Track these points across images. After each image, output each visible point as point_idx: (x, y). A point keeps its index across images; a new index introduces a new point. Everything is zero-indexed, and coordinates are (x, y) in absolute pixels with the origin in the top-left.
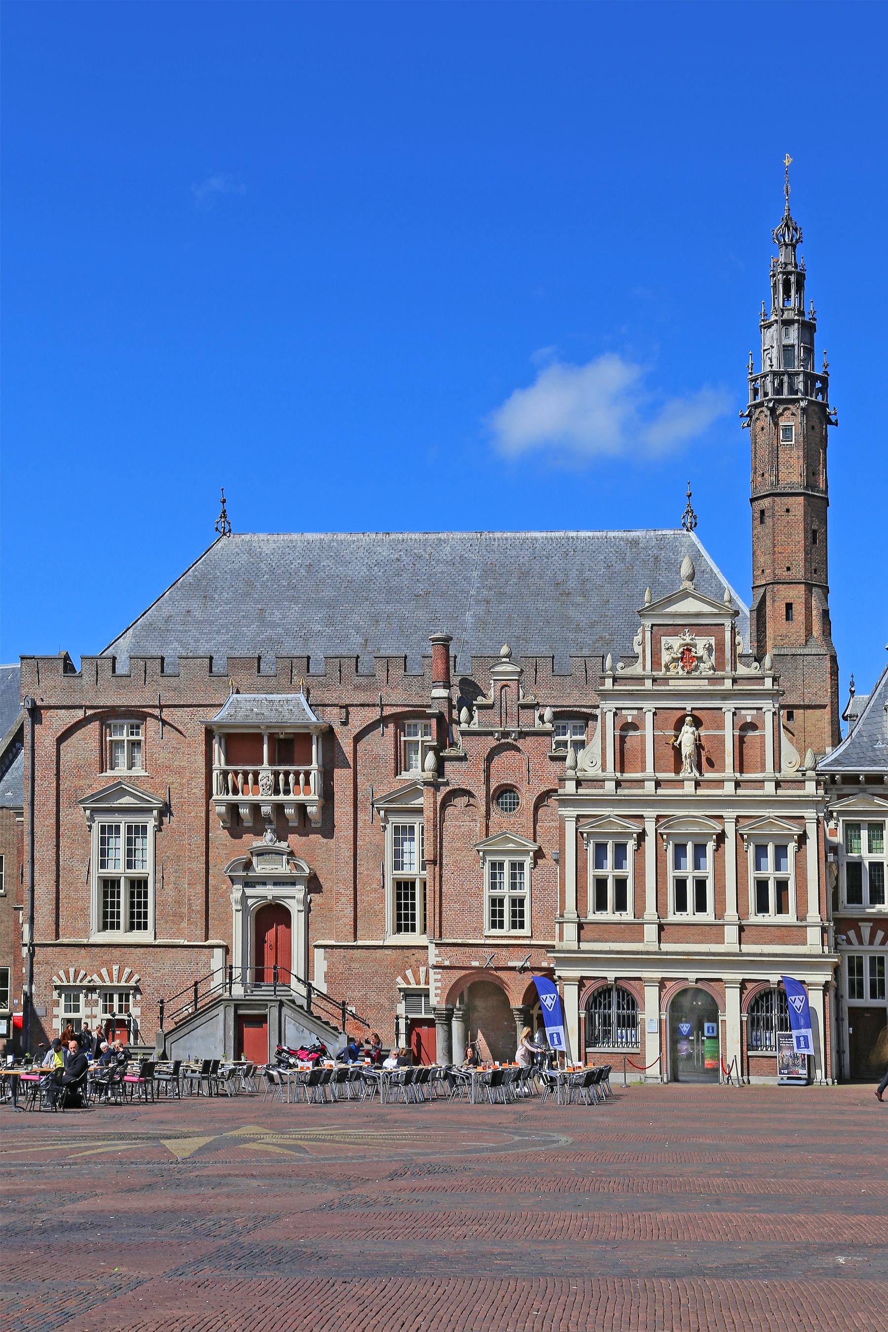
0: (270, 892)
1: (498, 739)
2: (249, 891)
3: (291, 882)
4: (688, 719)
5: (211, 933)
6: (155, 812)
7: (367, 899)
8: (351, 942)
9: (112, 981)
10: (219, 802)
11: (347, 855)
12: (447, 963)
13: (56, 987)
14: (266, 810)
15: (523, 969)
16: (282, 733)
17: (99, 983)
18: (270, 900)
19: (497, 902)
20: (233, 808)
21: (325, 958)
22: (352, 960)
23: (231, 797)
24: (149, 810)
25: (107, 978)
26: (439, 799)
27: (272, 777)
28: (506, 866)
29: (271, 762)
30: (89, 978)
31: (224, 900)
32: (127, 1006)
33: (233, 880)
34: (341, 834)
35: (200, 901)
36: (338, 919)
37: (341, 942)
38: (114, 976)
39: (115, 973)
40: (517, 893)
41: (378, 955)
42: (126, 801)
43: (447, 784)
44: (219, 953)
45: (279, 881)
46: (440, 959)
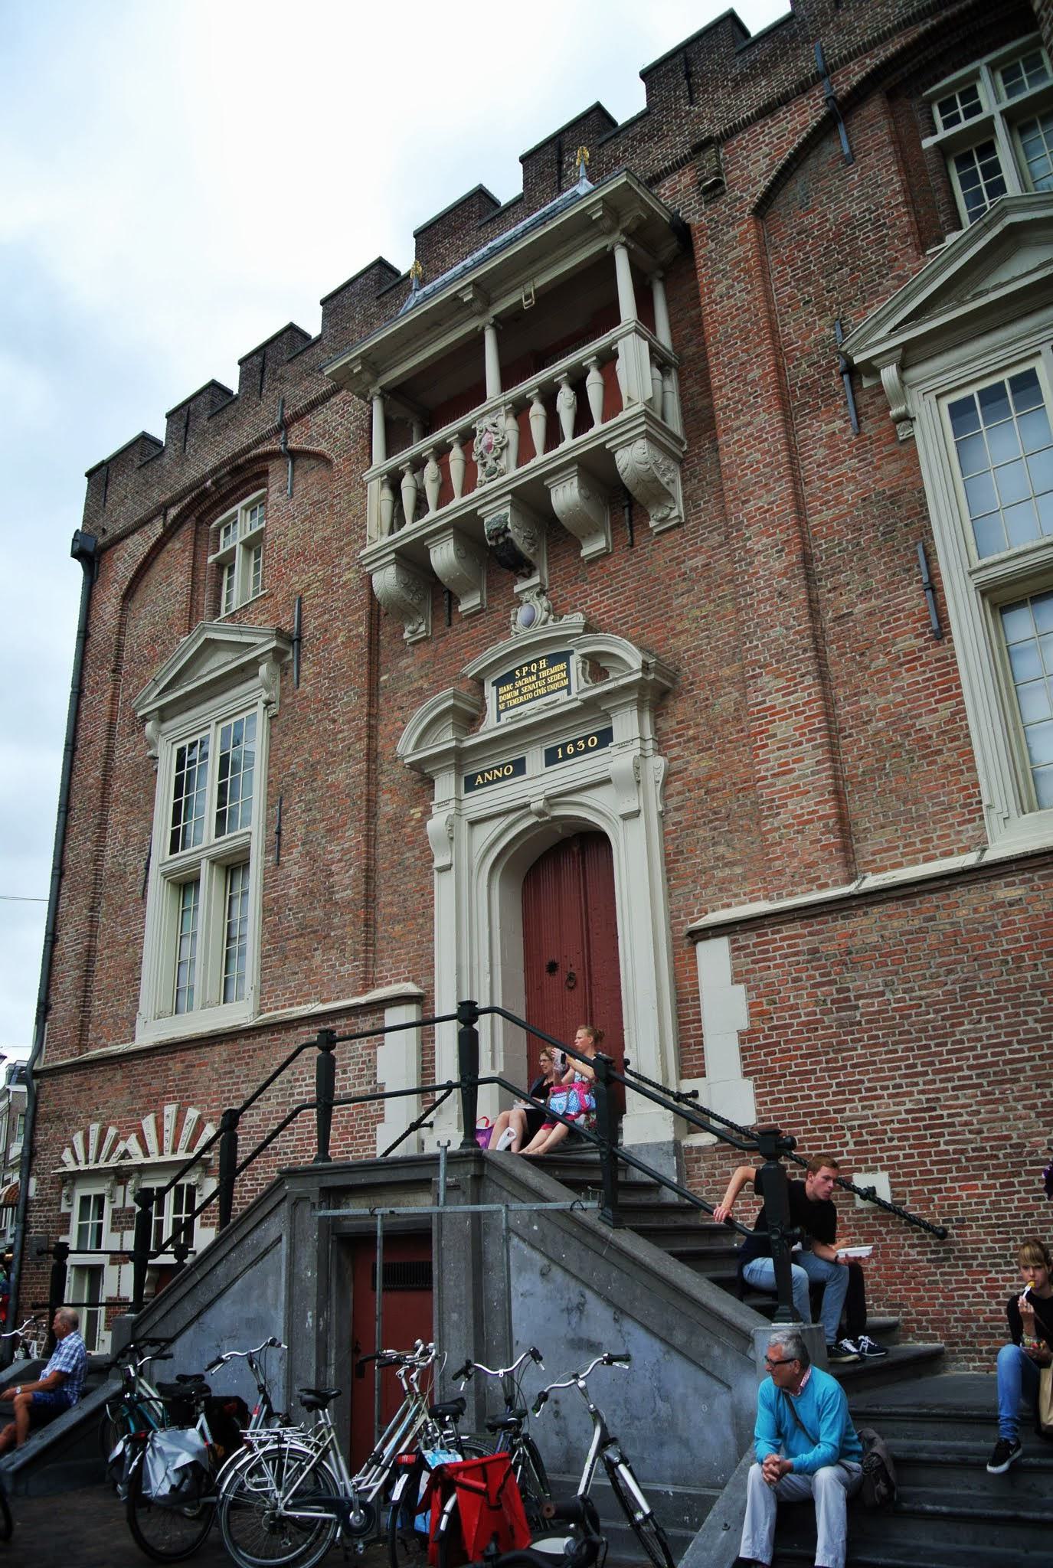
7: (881, 701)
8: (836, 883)
11: (778, 566)
16: (527, 297)
17: (139, 1159)
18: (540, 813)
21: (738, 977)
22: (849, 959)
31: (417, 852)
34: (750, 507)
35: (351, 872)
36: (775, 809)
37: (791, 895)
38: (166, 1135)
39: (169, 1125)
41: (963, 912)
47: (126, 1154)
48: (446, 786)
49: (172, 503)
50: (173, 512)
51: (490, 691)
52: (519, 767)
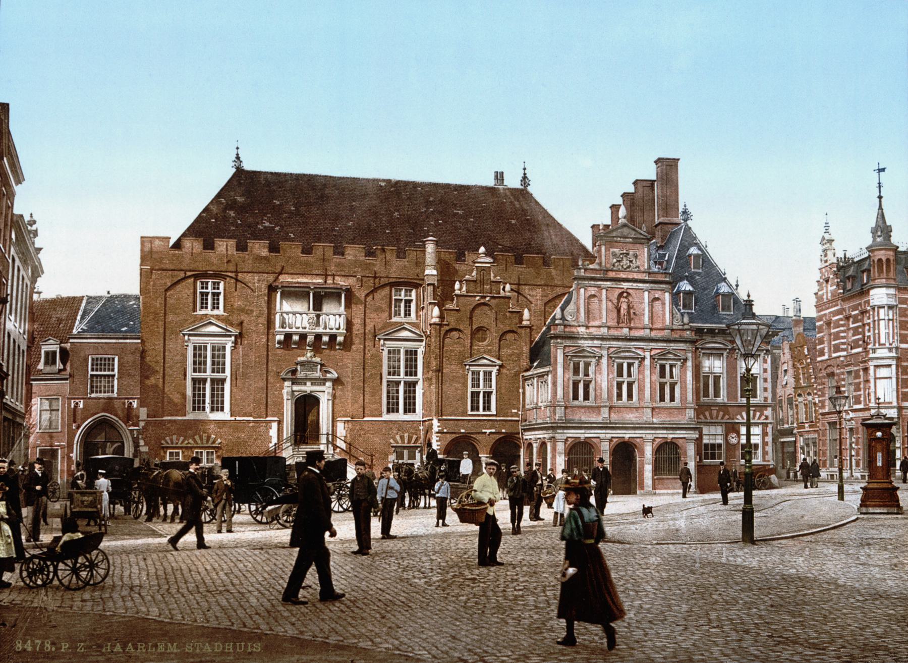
0: (308, 388)
2: (295, 388)
3: (323, 381)
4: (625, 294)
5: (269, 413)
6: (233, 338)
9: (202, 443)
10: (280, 333)
12: (445, 431)
13: (163, 448)
14: (310, 338)
15: (491, 433)
19: (475, 395)
20: (288, 336)
23: (287, 329)
24: (230, 336)
25: (199, 442)
26: (443, 333)
27: (315, 319)
28: (482, 374)
29: (314, 309)
30: (186, 442)
40: (488, 390)
43: (448, 325)
44: (275, 426)
45: (315, 381)
47: (189, 443)
48: (287, 384)
49: (190, 271)
51: (299, 368)
52: (305, 384)
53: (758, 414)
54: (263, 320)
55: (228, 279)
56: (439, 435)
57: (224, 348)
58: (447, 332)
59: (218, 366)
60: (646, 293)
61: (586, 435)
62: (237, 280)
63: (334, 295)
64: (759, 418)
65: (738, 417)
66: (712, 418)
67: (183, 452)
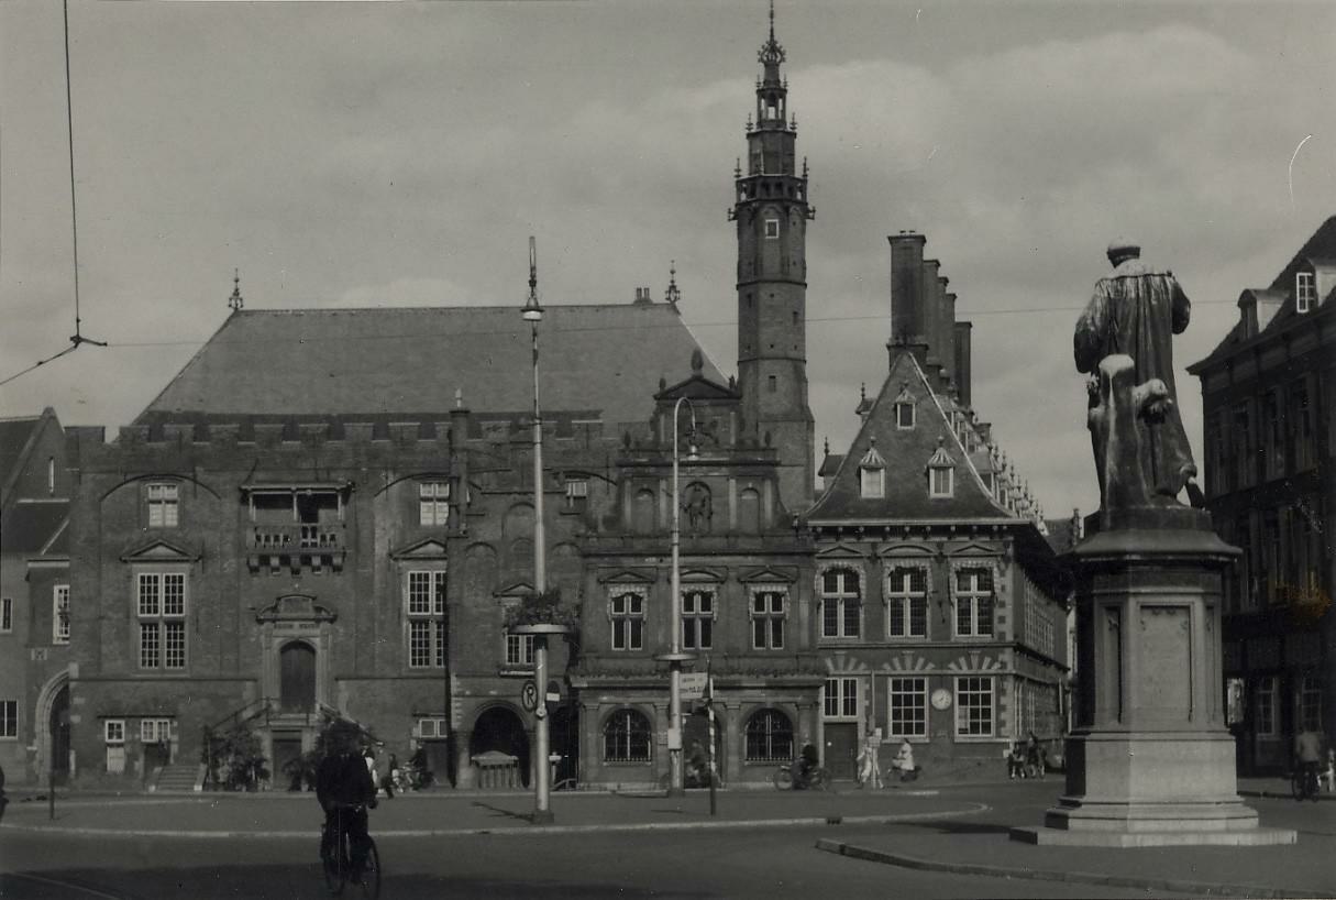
0: (296, 631)
1: (515, 499)
2: (275, 632)
12: (468, 693)
24: (187, 561)
32: (166, 733)
33: (260, 622)
42: (161, 551)
46: (460, 690)
49: (133, 472)
50: (128, 477)
53: (987, 660)
54: (230, 537)
55: (186, 481)
56: (460, 699)
57: (181, 578)
58: (469, 547)
59: (174, 603)
60: (733, 482)
61: (631, 700)
62: (194, 480)
63: (329, 501)
64: (989, 668)
65: (952, 666)
66: (904, 668)
67: (126, 724)
